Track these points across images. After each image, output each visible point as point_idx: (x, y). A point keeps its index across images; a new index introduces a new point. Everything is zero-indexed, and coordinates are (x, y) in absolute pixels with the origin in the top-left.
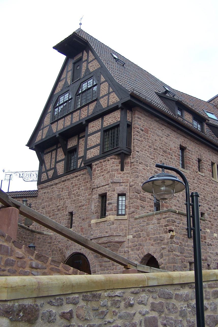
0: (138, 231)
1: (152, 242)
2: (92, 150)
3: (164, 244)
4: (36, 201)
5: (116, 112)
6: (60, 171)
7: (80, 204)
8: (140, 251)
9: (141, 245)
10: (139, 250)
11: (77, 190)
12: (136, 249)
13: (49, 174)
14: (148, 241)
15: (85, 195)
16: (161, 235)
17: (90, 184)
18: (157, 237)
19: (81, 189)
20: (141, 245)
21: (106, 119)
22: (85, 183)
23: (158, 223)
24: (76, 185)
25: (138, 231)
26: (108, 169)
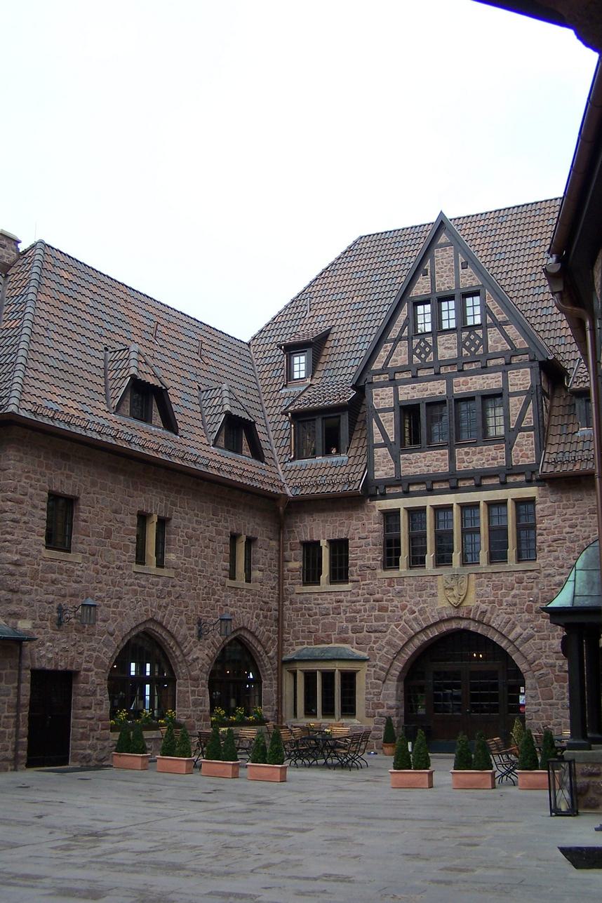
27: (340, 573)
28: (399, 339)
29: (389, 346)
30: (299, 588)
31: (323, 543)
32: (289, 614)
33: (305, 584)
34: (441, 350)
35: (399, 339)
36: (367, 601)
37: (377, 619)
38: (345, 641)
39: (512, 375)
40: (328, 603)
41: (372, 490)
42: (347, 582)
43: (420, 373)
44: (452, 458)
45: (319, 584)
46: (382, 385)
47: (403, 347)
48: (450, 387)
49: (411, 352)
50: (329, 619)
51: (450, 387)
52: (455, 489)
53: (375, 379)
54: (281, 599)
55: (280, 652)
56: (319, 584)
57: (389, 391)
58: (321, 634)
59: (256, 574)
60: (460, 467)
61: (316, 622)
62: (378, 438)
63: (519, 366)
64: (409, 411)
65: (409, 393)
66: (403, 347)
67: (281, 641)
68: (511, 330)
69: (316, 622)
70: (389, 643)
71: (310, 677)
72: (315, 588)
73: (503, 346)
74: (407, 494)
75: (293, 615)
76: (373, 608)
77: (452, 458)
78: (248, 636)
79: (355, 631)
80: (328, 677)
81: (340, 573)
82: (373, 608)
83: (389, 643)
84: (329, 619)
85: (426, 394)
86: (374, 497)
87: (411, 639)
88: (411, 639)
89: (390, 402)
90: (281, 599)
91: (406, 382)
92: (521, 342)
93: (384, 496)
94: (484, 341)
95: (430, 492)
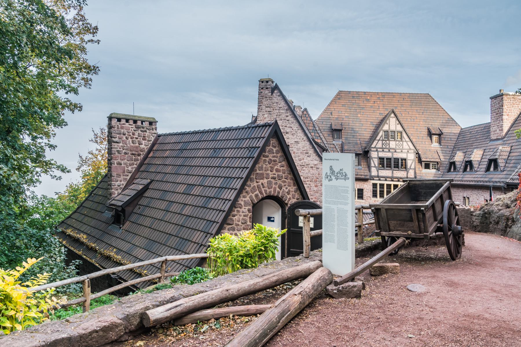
28: (379, 140)
29: (377, 141)
34: (391, 145)
35: (379, 140)
39: (409, 155)
41: (372, 178)
43: (385, 150)
44: (393, 173)
46: (374, 151)
47: (380, 142)
48: (393, 155)
49: (383, 144)
51: (393, 155)
52: (392, 181)
53: (372, 149)
57: (376, 153)
60: (395, 175)
62: (372, 165)
63: (411, 153)
64: (381, 159)
65: (381, 155)
66: (380, 142)
68: (410, 143)
73: (407, 147)
74: (380, 180)
77: (393, 173)
85: (386, 156)
86: (371, 179)
89: (376, 156)
91: (381, 152)
92: (412, 147)
93: (373, 179)
94: (402, 145)
95: (386, 180)
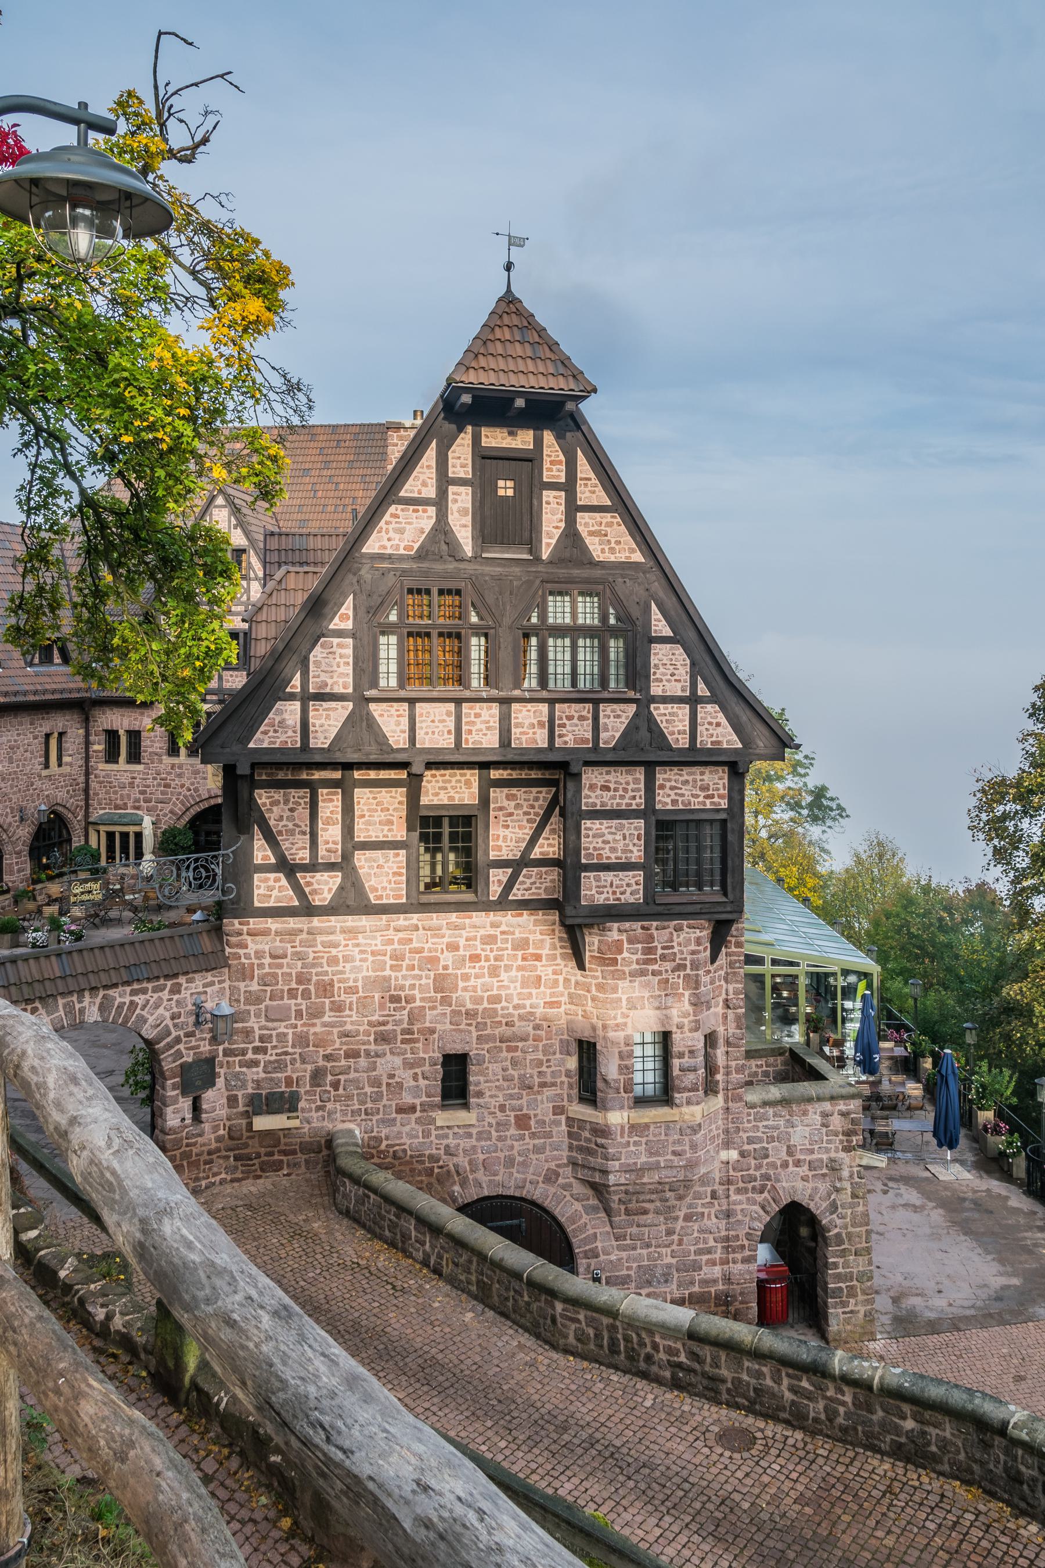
0: (760, 1140)
1: (804, 1170)
2: (608, 876)
3: (840, 1179)
4: (220, 982)
5: (711, 772)
6: (384, 889)
7: (508, 1032)
8: (766, 1194)
9: (769, 1179)
10: (762, 1192)
11: (487, 979)
12: (754, 1188)
13: (309, 884)
14: (791, 1168)
15: (528, 1003)
16: (833, 1155)
17: (550, 970)
18: (821, 1160)
19: (504, 976)
20: (769, 1179)
21: (669, 780)
22: (524, 959)
23: (823, 1125)
24: (475, 958)
25: (760, 1140)
26: (678, 956)
27: (134, 757)
30: (102, 766)
31: (121, 732)
32: (93, 785)
33: (107, 762)
36: (155, 779)
37: (163, 793)
38: (138, 808)
40: (125, 779)
42: (139, 763)
45: (117, 762)
50: (126, 792)
54: (87, 774)
55: (87, 815)
56: (117, 762)
58: (119, 802)
59: (66, 759)
61: (115, 793)
67: (87, 805)
69: (115, 793)
70: (171, 812)
71: (110, 836)
72: (114, 767)
75: (97, 786)
76: (159, 785)
78: (60, 809)
79: (145, 801)
80: (125, 836)
81: (134, 757)
82: (159, 785)
83: (171, 812)
84: (126, 792)
87: (188, 809)
88: (188, 809)
90: (87, 774)
